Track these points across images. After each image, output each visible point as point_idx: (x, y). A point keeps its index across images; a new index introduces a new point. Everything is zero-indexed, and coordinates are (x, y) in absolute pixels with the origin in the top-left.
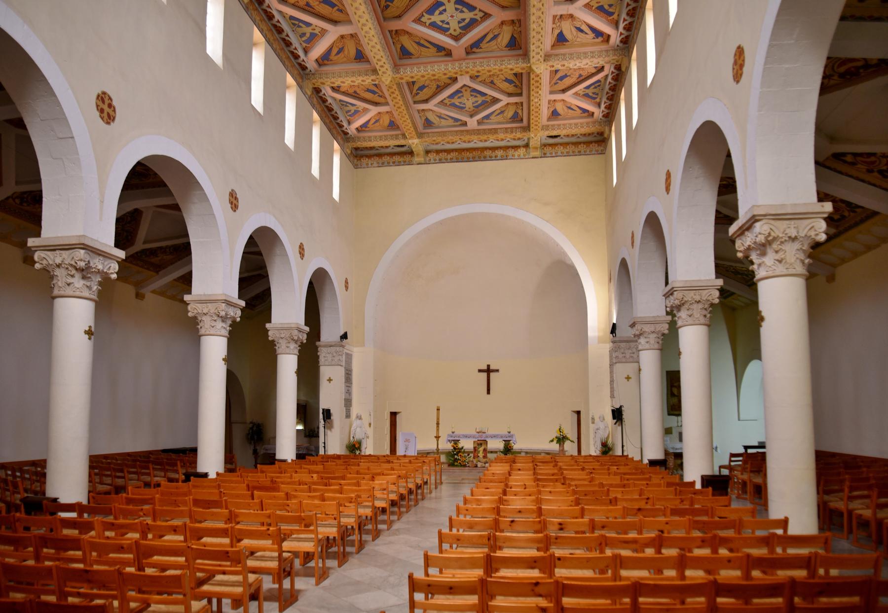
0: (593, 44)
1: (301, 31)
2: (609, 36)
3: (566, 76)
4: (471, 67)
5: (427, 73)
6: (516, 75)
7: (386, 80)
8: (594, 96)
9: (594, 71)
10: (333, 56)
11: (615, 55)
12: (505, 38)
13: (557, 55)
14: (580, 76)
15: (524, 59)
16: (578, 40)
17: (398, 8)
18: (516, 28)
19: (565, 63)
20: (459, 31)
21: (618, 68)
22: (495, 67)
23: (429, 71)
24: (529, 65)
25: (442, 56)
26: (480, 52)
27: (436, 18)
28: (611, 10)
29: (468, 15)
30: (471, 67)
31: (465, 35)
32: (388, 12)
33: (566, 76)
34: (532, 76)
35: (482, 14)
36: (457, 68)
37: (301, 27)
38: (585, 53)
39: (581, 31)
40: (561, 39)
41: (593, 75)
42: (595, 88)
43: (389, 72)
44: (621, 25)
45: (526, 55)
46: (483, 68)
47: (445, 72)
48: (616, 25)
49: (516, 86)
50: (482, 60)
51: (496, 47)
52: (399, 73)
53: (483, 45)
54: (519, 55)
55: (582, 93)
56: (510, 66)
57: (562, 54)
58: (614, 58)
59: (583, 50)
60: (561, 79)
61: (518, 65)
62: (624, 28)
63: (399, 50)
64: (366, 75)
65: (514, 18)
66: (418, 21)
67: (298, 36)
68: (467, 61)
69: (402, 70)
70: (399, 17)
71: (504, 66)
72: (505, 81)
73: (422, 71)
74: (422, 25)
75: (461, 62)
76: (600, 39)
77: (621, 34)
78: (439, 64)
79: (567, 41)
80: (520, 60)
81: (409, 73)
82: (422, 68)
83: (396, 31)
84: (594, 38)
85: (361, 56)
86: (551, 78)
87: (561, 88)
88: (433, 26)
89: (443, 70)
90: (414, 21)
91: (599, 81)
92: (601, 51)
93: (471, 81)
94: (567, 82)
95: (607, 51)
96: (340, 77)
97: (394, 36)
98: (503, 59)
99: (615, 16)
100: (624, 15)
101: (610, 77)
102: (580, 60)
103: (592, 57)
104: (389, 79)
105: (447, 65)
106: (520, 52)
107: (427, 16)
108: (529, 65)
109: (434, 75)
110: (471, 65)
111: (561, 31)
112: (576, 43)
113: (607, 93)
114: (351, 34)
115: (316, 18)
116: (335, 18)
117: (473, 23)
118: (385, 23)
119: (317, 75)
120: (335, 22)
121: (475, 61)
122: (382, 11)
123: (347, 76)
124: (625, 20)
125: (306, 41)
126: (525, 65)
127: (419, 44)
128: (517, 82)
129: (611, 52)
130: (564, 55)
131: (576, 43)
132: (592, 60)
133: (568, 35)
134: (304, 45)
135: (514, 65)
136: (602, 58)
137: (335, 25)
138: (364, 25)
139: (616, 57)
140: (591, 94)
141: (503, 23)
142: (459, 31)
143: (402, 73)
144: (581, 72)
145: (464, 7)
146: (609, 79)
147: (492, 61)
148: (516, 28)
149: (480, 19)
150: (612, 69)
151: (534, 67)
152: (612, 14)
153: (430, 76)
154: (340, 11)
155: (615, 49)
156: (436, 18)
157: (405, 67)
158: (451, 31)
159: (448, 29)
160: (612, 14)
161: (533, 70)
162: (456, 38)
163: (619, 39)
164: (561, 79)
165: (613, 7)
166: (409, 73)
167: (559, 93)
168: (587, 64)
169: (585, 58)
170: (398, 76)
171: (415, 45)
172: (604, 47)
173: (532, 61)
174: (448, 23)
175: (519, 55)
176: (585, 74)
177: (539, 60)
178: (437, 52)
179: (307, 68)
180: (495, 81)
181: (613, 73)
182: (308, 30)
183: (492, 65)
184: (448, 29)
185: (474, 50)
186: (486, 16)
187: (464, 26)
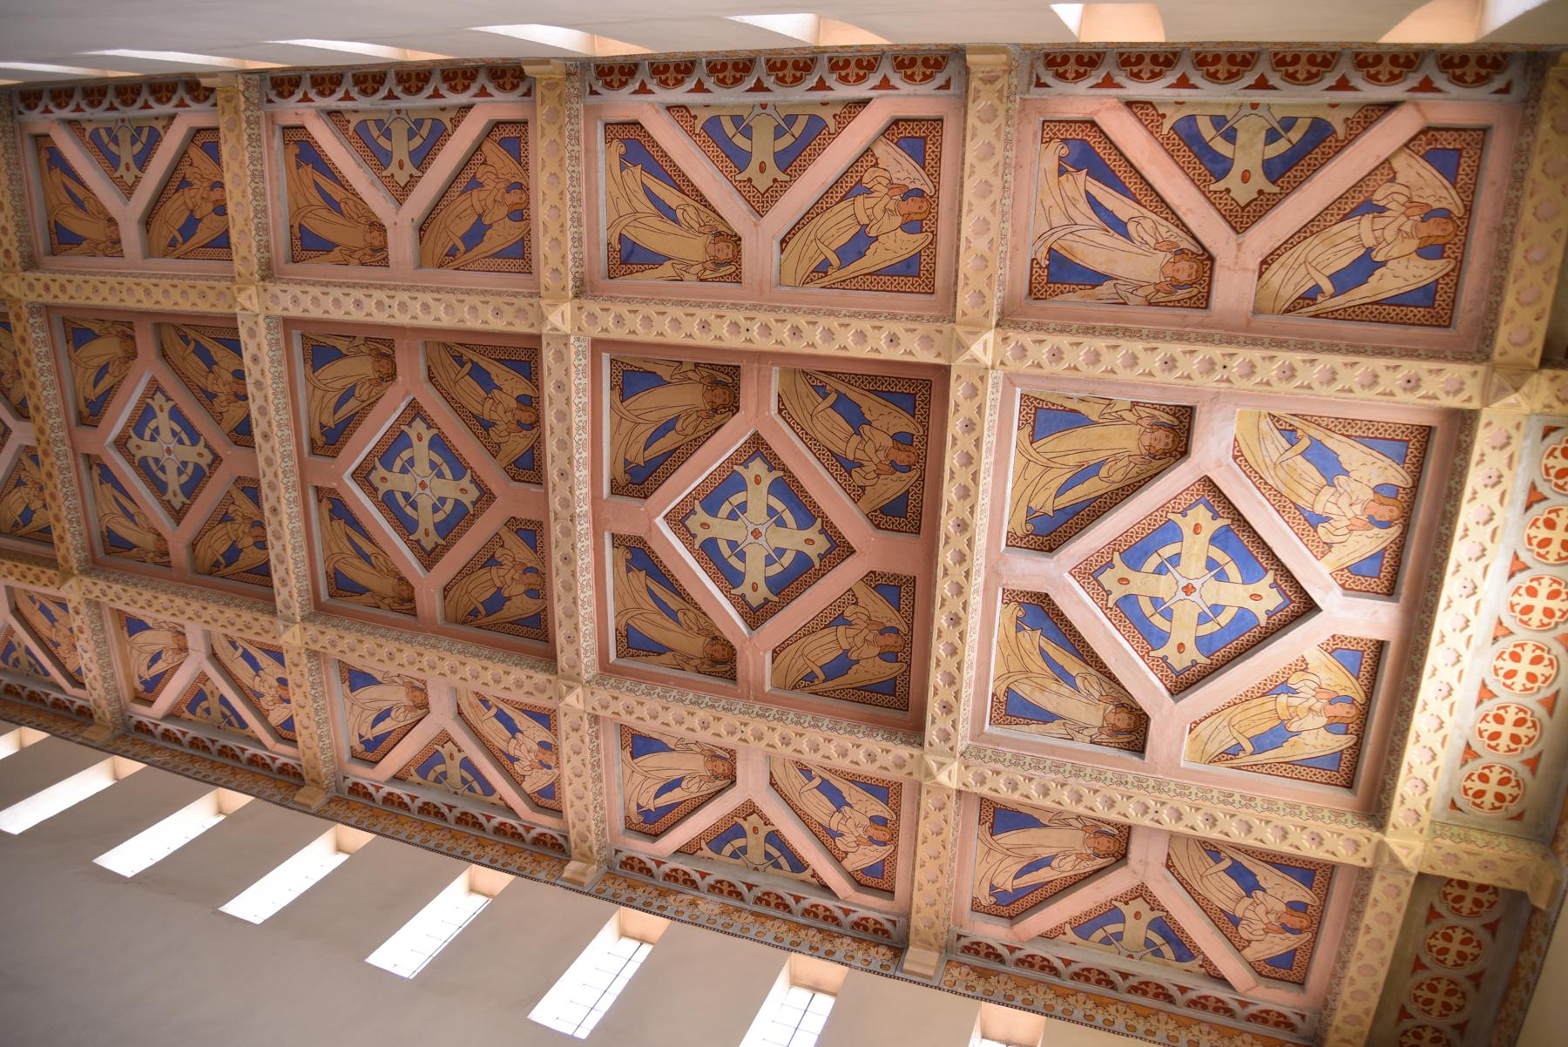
0: (129, 677)
1: (124, 136)
2: (150, 703)
3: (52, 619)
4: (59, 463)
5: (38, 375)
6: (47, 530)
7: (12, 286)
8: (11, 661)
9: (71, 667)
10: (57, 176)
11: (112, 714)
12: (125, 530)
13: (100, 617)
14: (57, 645)
15: (86, 560)
16: (135, 653)
17: (184, 359)
18: (151, 555)
19: (87, 634)
20: (139, 454)
21: (84, 715)
22: (64, 509)
23: (43, 379)
24: (76, 572)
25: (77, 405)
26: (92, 478)
27: (163, 420)
28: (199, 710)
29: (173, 481)
30: (59, 463)
31: (131, 461)
32: (171, 338)
33: (52, 619)
34: (50, 572)
35: (177, 504)
36: (53, 435)
37: (133, 143)
38: (110, 665)
39: (156, 658)
40: (135, 626)
41: (61, 666)
42: (31, 665)
43: (32, 297)
44: (173, 727)
45: (93, 567)
46: (59, 487)
47: (44, 413)
48: (171, 716)
49: (16, 524)
50: (75, 482)
51: (107, 511)
52: (31, 314)
53: (108, 488)
54: (92, 551)
55: (14, 640)
56: (68, 538)
57: (103, 625)
58: (108, 714)
59: (116, 659)
60: (43, 609)
61: (72, 553)
62: (167, 730)
63: (86, 325)
64: (20, 241)
65: (173, 557)
66: (155, 388)
67: (112, 125)
68: (70, 454)
69: (38, 320)
70: (164, 355)
71: (67, 526)
72: (27, 507)
73: (40, 365)
74: (148, 389)
75: (68, 442)
76: (141, 688)
77: (156, 725)
78: (59, 398)
79: (132, 632)
80: (83, 554)
81: (34, 335)
82: (47, 364)
83: (132, 338)
84: (140, 677)
85: (63, 239)
86: (44, 595)
87: (21, 605)
88: (144, 415)
89: (48, 408)
90: (154, 381)
91: (47, 674)
92: (116, 690)
93: (20, 446)
94: (40, 622)
95: (118, 699)
96: (10, 180)
97: (119, 328)
98: (82, 521)
99: (187, 715)
100: (192, 733)
101: (61, 697)
102: (95, 659)
103: (104, 678)
104: (16, 294)
105: (58, 413)
106: (100, 552)
107: (168, 406)
108: (76, 572)
109: (28, 363)
110: (63, 462)
111: (149, 628)
112: (128, 648)
113: (23, 688)
114: (119, 241)
115: (156, 190)
116: (156, 224)
117: (159, 487)
118: (149, 326)
119: (10, 124)
120: (147, 221)
121: (73, 469)
122: (174, 326)
123: (13, 196)
124: (184, 734)
125: (95, 135)
126: (74, 563)
127: (102, 371)
128: (27, 528)
129: (117, 706)
130: (102, 630)
131: (128, 648)
132: (99, 679)
133: (142, 637)
134: (89, 128)
135: (71, 543)
136: (103, 694)
137: (140, 222)
138: (148, 292)
139: (108, 716)
140: (14, 655)
141: (159, 535)
142: (139, 454)
143: (31, 321)
144: (64, 647)
145: (191, 478)
146: (54, 695)
147: (78, 502)
148: (151, 555)
149: (165, 498)
150: (79, 702)
151: (72, 582)
152: (193, 712)
153: (30, 377)
154: (173, 243)
155: (123, 715)
156: (163, 420)
157: (46, 327)
158: (135, 440)
159: (141, 437)
160: (193, 712)
161: (64, 580)
162: (121, 444)
163: (145, 720)
164: (43, 609)
165: (205, 715)
166: (34, 335)
167: (10, 602)
168: (86, 658)
169: (102, 667)
170: (25, 313)
171: (102, 361)
172: (126, 694)
173: (87, 581)
174: (153, 439)
175: (92, 551)
176: (62, 652)
177: (90, 592)
178: (86, 400)
179: (30, 108)
180: (23, 491)
181: (72, 703)
182: (126, 152)
183: (67, 503)
184: (141, 437)
185: (96, 471)
186: (178, 515)
187: (149, 467)
